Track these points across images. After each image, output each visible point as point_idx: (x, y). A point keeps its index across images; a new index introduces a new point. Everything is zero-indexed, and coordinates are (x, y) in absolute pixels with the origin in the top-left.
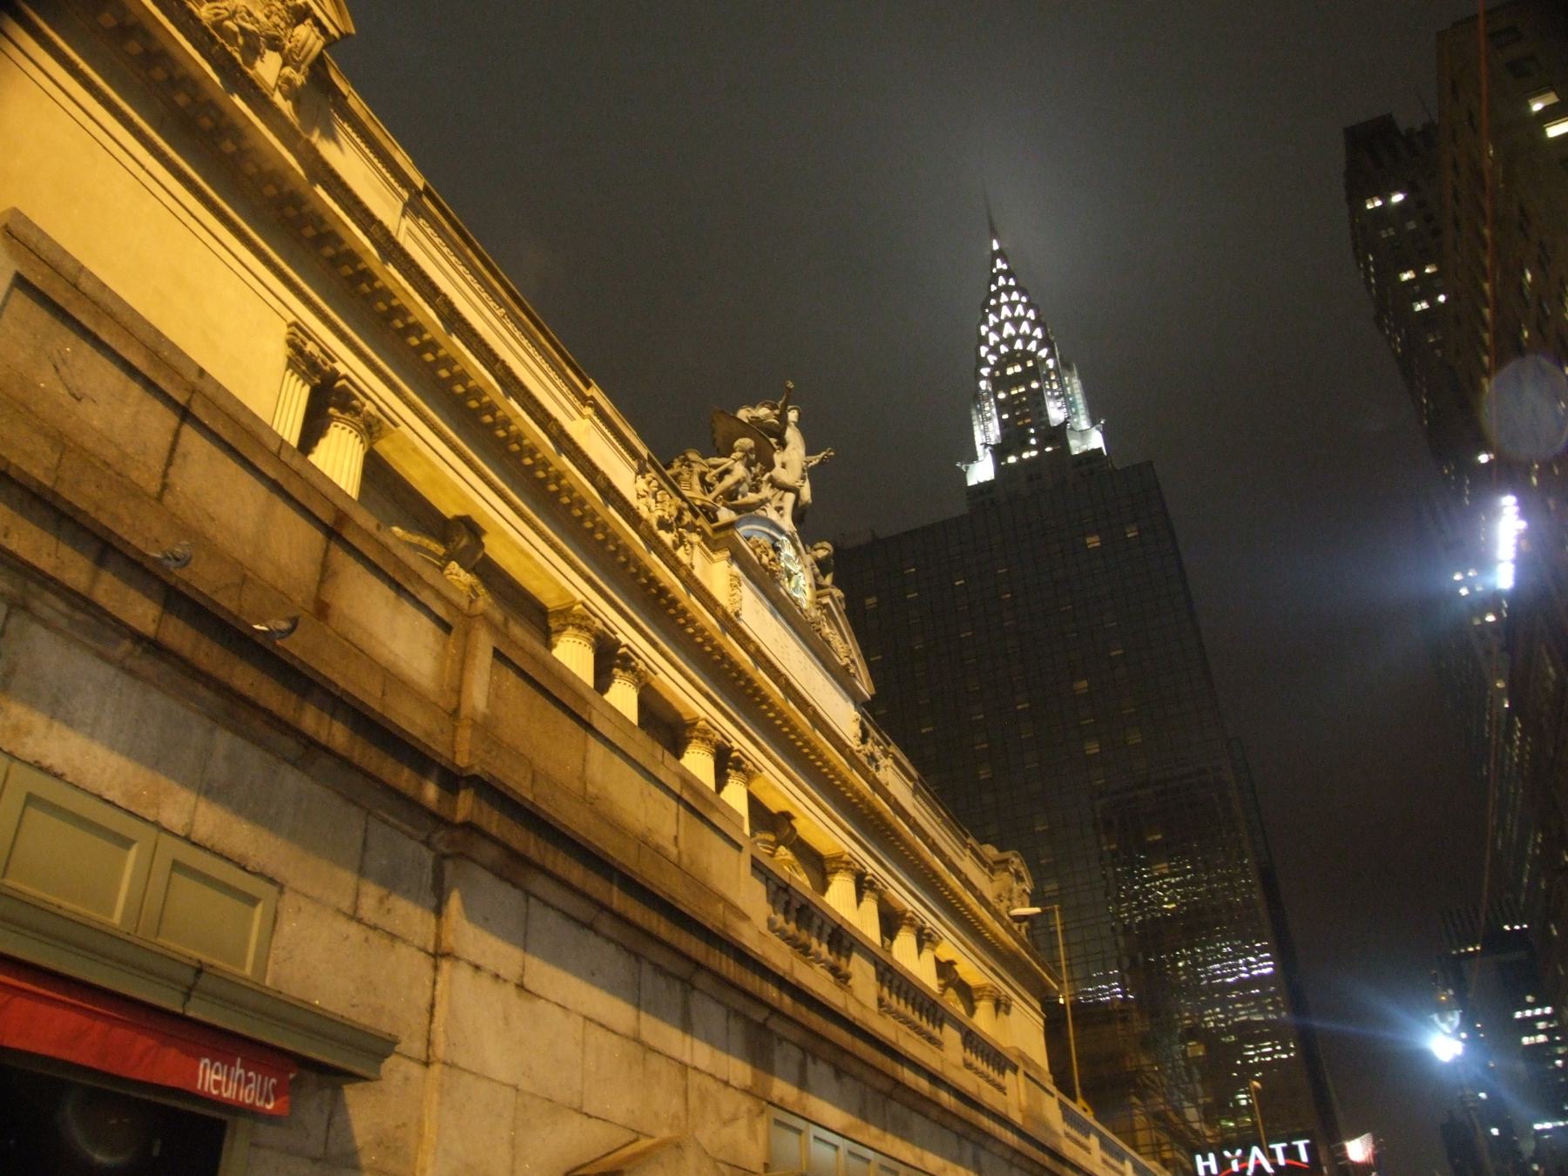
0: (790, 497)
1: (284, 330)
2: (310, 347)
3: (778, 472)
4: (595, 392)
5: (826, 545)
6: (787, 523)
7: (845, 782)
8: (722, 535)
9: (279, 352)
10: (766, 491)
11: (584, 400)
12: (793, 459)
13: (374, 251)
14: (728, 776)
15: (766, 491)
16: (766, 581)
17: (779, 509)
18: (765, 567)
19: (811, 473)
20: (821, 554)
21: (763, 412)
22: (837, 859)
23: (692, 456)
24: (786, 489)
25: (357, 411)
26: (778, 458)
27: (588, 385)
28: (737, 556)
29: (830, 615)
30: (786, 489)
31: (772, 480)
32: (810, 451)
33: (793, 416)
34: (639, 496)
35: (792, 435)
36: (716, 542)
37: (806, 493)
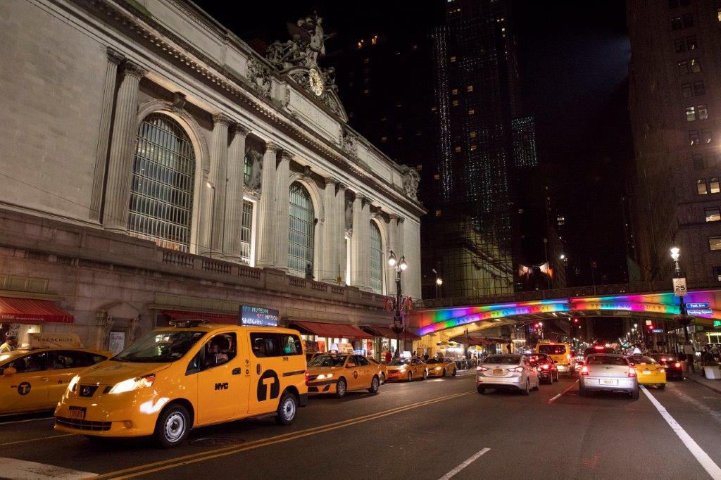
0: (316, 54)
1: (106, 49)
2: (116, 54)
3: (313, 45)
4: (230, 35)
5: (333, 68)
6: (314, 64)
7: (332, 154)
8: (284, 75)
9: (103, 57)
10: (308, 51)
11: (225, 38)
12: (317, 40)
13: (132, 16)
14: (282, 158)
15: (308, 51)
16: (303, 89)
17: (312, 58)
18: (300, 85)
19: (327, 43)
20: (331, 71)
21: (308, 20)
22: (329, 178)
23: (277, 43)
24: (314, 50)
25: (134, 70)
26: (313, 38)
27: (226, 32)
28: (288, 82)
29: (331, 95)
30: (315, 51)
31: (310, 47)
32: (325, 33)
33: (319, 21)
34: (249, 68)
35: (318, 29)
36: (281, 78)
37: (323, 51)
